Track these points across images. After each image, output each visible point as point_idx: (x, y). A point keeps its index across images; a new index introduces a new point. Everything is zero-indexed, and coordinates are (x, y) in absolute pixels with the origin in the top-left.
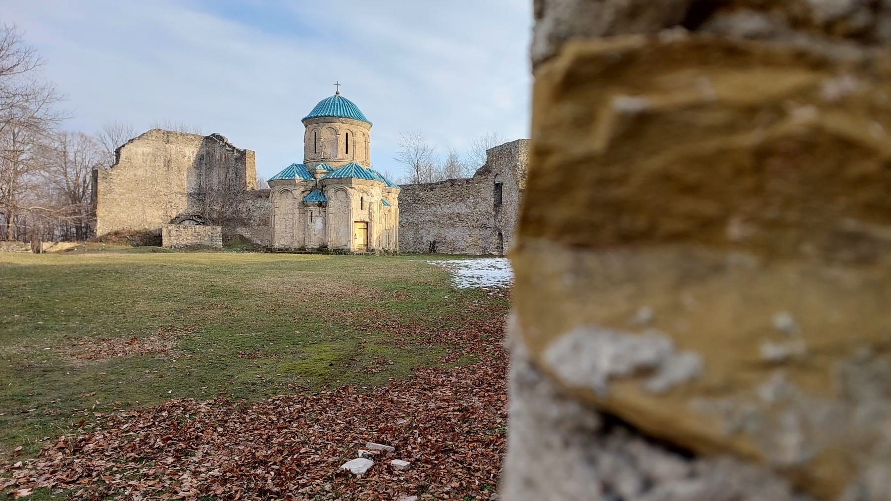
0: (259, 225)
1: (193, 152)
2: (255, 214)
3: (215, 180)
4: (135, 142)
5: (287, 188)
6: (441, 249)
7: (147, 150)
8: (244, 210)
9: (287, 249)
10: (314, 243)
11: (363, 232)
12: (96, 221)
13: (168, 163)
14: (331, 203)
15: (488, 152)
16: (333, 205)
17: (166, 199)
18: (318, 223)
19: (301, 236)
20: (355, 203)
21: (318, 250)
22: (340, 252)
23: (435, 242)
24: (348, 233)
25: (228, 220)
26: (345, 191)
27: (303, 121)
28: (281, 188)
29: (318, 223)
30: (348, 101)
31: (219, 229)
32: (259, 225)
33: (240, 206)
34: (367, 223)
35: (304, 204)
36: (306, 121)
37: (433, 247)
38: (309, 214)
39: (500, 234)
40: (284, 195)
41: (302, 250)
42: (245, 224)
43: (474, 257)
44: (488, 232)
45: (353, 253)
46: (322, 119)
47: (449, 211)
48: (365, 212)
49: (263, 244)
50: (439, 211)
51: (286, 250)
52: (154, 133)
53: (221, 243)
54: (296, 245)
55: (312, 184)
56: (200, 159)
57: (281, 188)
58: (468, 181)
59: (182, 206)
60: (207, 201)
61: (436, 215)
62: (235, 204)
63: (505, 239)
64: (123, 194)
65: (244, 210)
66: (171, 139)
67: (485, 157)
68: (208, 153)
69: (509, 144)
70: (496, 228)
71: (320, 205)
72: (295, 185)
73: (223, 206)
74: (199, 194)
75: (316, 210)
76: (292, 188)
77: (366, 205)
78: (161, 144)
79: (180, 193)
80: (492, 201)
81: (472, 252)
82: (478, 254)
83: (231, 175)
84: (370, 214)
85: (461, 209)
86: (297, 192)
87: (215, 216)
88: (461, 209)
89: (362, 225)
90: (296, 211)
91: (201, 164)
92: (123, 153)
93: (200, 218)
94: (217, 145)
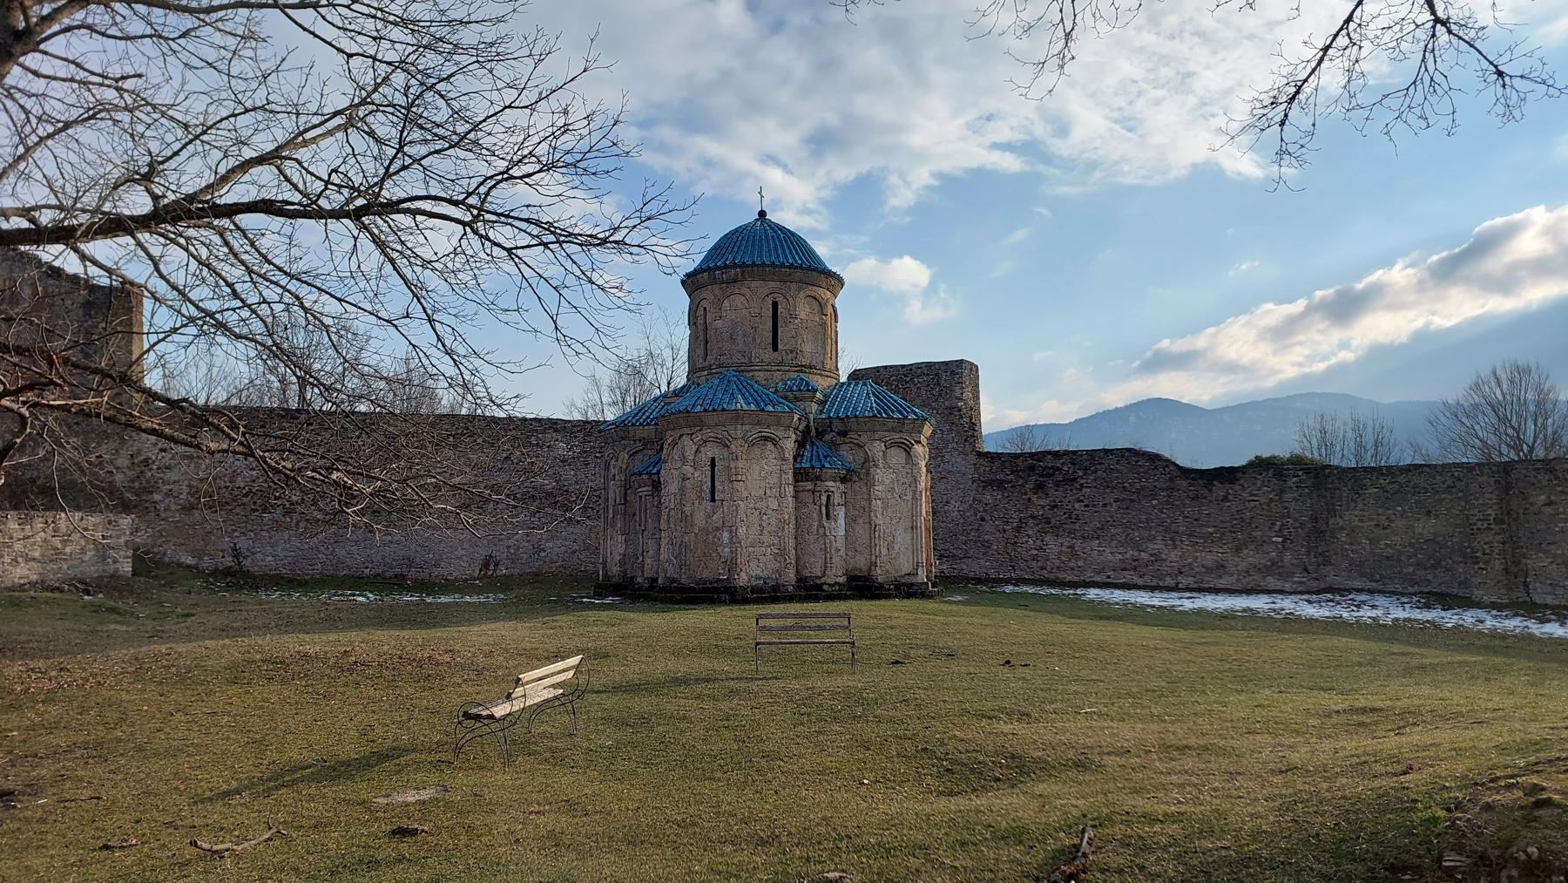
0: (188, 509)
2: (172, 476)
5: (767, 432)
8: (123, 461)
9: (776, 588)
28: (754, 433)
32: (188, 509)
35: (800, 475)
38: (824, 498)
40: (756, 451)
41: (810, 590)
46: (798, 274)
49: (206, 563)
57: (754, 433)
69: (929, 365)
71: (843, 480)
76: (780, 433)
86: (789, 445)
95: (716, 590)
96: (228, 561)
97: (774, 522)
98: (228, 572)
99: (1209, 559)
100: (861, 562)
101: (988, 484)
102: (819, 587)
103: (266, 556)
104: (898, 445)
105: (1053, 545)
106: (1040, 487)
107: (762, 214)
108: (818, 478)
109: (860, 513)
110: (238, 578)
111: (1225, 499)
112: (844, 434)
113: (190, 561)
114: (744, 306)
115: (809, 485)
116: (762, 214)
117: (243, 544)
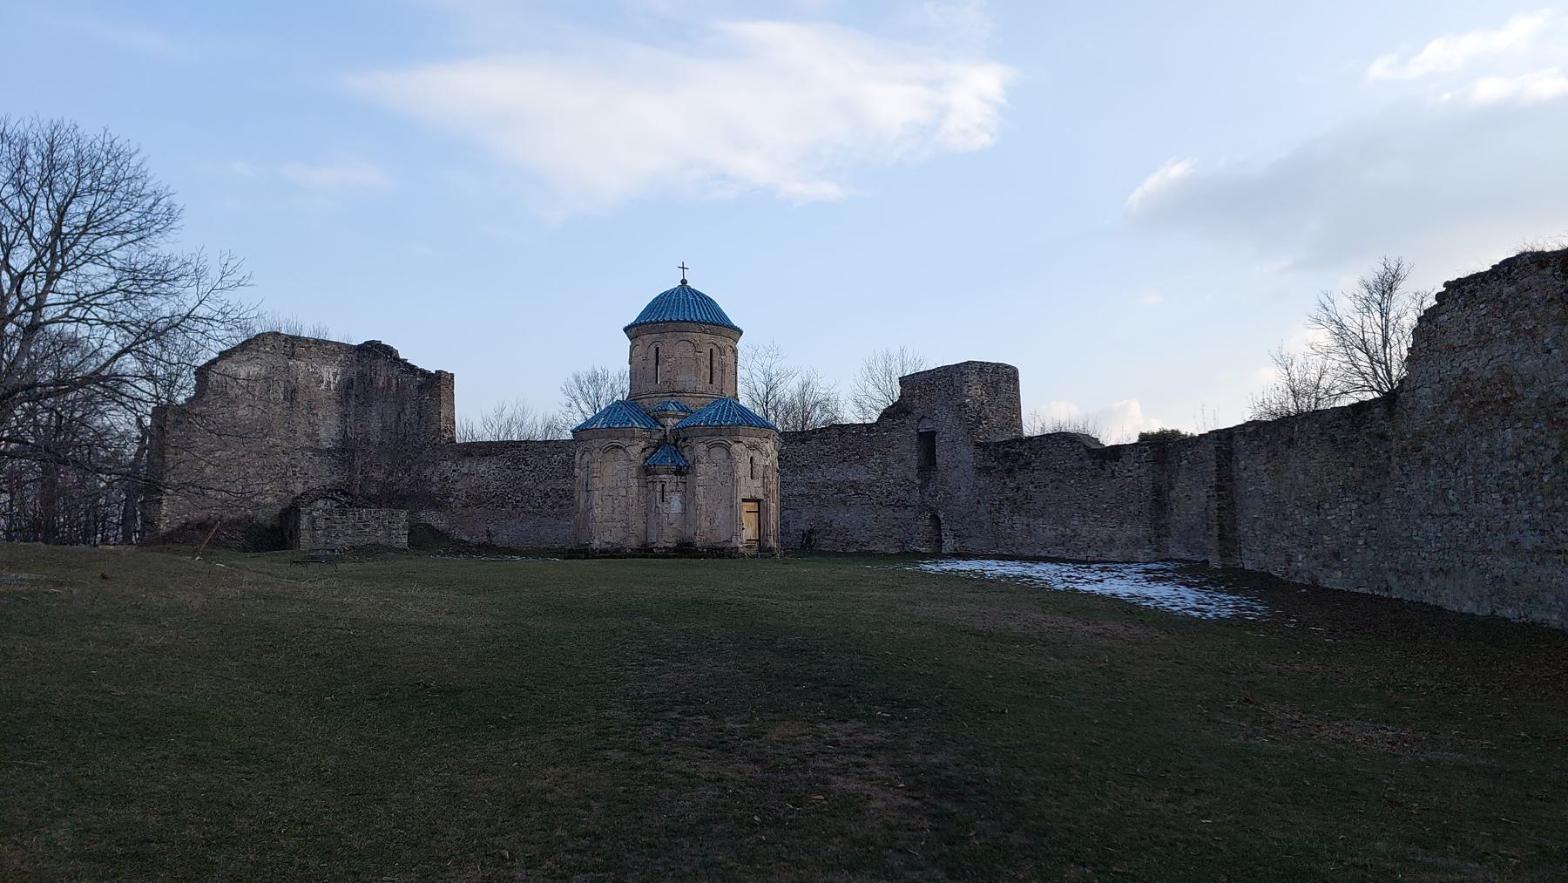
0: (466, 506)
1: (335, 375)
2: (458, 486)
3: (376, 425)
4: (236, 357)
5: (616, 442)
6: (826, 544)
7: (254, 370)
8: (435, 479)
9: (618, 551)
10: (668, 539)
11: (753, 517)
12: (159, 502)
13: (292, 394)
14: (701, 468)
15: (903, 381)
16: (705, 471)
17: (286, 460)
18: (675, 504)
19: (640, 526)
20: (743, 469)
21: (675, 550)
22: (721, 552)
23: (811, 532)
24: (735, 521)
25: (402, 498)
26: (727, 448)
27: (626, 330)
29: (675, 504)
30: (707, 298)
31: (403, 514)
32: (466, 506)
33: (427, 472)
34: (758, 501)
35: (647, 471)
36: (632, 331)
37: (809, 540)
38: (659, 487)
39: (935, 518)
40: (610, 456)
42: (436, 504)
43: (885, 557)
44: (909, 514)
45: (743, 555)
47: (837, 478)
48: (758, 483)
49: (475, 540)
50: (818, 478)
51: (612, 553)
52: (270, 340)
53: (405, 540)
54: (633, 542)
55: (657, 436)
56: (346, 390)
58: (869, 427)
59: (324, 475)
60: (359, 463)
61: (812, 485)
62: (415, 468)
63: (945, 526)
64: (211, 451)
65: (435, 479)
66: (298, 350)
67: (898, 389)
68: (362, 376)
69: (946, 368)
70: (924, 507)
72: (633, 438)
73: (391, 474)
74: (343, 450)
75: (670, 480)
76: (627, 443)
77: (759, 471)
78: (279, 361)
79: (310, 449)
80: (913, 461)
81: (881, 548)
82: (892, 551)
83: (409, 414)
84: (764, 486)
85: (858, 474)
86: (635, 450)
87: (374, 491)
88: (858, 474)
89: (752, 506)
90: (634, 483)
91: (347, 394)
92: (213, 378)
93: (346, 494)
94: (381, 362)
95: (580, 551)
96: (485, 539)
97: (623, 504)
98: (479, 546)
99: (1104, 533)
100: (690, 532)
101: (983, 470)
102: (651, 550)
103: (503, 538)
104: (719, 445)
105: (1019, 522)
106: (1010, 471)
107: (684, 282)
108: (655, 473)
109: (688, 500)
110: (488, 549)
111: (1113, 476)
112: (685, 440)
113: (466, 538)
114: (677, 350)
115: (650, 478)
116: (684, 282)
117: (492, 528)
